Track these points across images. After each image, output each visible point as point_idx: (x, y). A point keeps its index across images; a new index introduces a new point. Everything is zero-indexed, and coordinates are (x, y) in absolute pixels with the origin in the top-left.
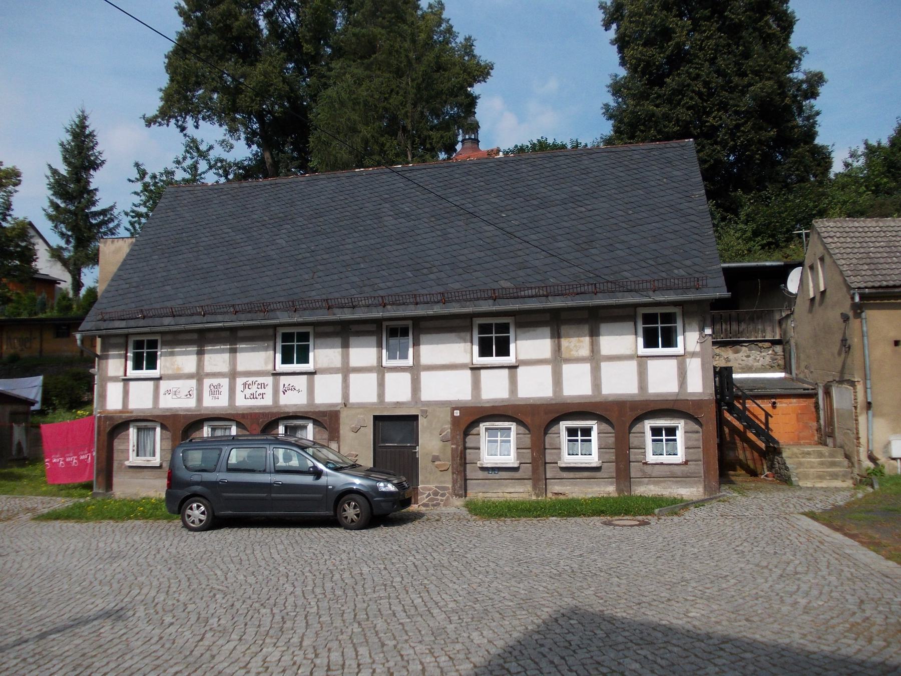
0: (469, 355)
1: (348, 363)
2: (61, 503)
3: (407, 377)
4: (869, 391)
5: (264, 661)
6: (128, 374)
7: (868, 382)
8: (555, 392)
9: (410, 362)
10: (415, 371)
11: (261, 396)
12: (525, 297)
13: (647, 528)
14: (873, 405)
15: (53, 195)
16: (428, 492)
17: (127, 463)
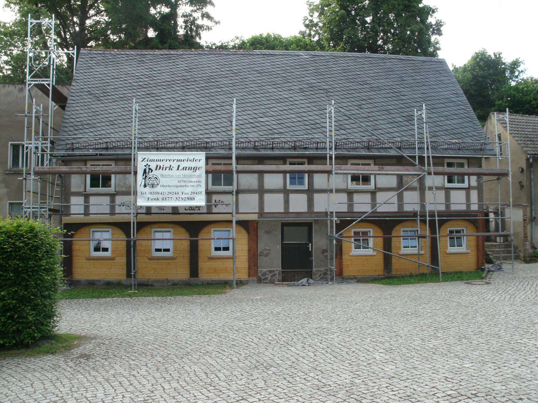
0: (346, 183)
1: (263, 186)
2: (340, 282)
3: (304, 197)
4: (533, 211)
5: (393, 377)
6: (87, 190)
7: (533, 206)
8: (399, 208)
9: (466, 185)
10: (311, 192)
11: (198, 209)
12: (386, 148)
13: (490, 285)
14: (536, 218)
15: (41, 23)
16: (320, 273)
17: (351, 254)
